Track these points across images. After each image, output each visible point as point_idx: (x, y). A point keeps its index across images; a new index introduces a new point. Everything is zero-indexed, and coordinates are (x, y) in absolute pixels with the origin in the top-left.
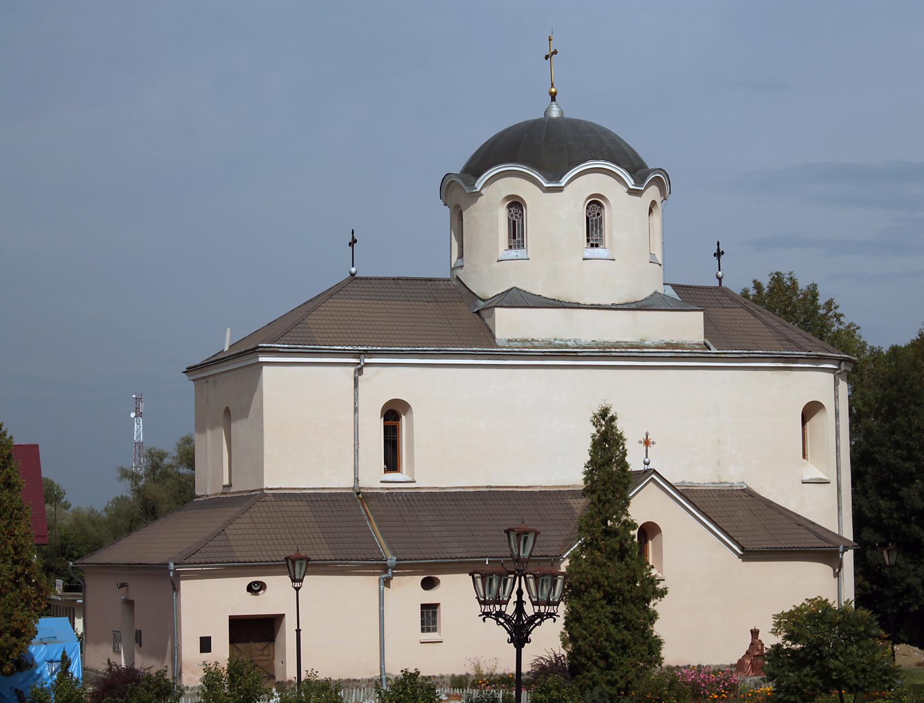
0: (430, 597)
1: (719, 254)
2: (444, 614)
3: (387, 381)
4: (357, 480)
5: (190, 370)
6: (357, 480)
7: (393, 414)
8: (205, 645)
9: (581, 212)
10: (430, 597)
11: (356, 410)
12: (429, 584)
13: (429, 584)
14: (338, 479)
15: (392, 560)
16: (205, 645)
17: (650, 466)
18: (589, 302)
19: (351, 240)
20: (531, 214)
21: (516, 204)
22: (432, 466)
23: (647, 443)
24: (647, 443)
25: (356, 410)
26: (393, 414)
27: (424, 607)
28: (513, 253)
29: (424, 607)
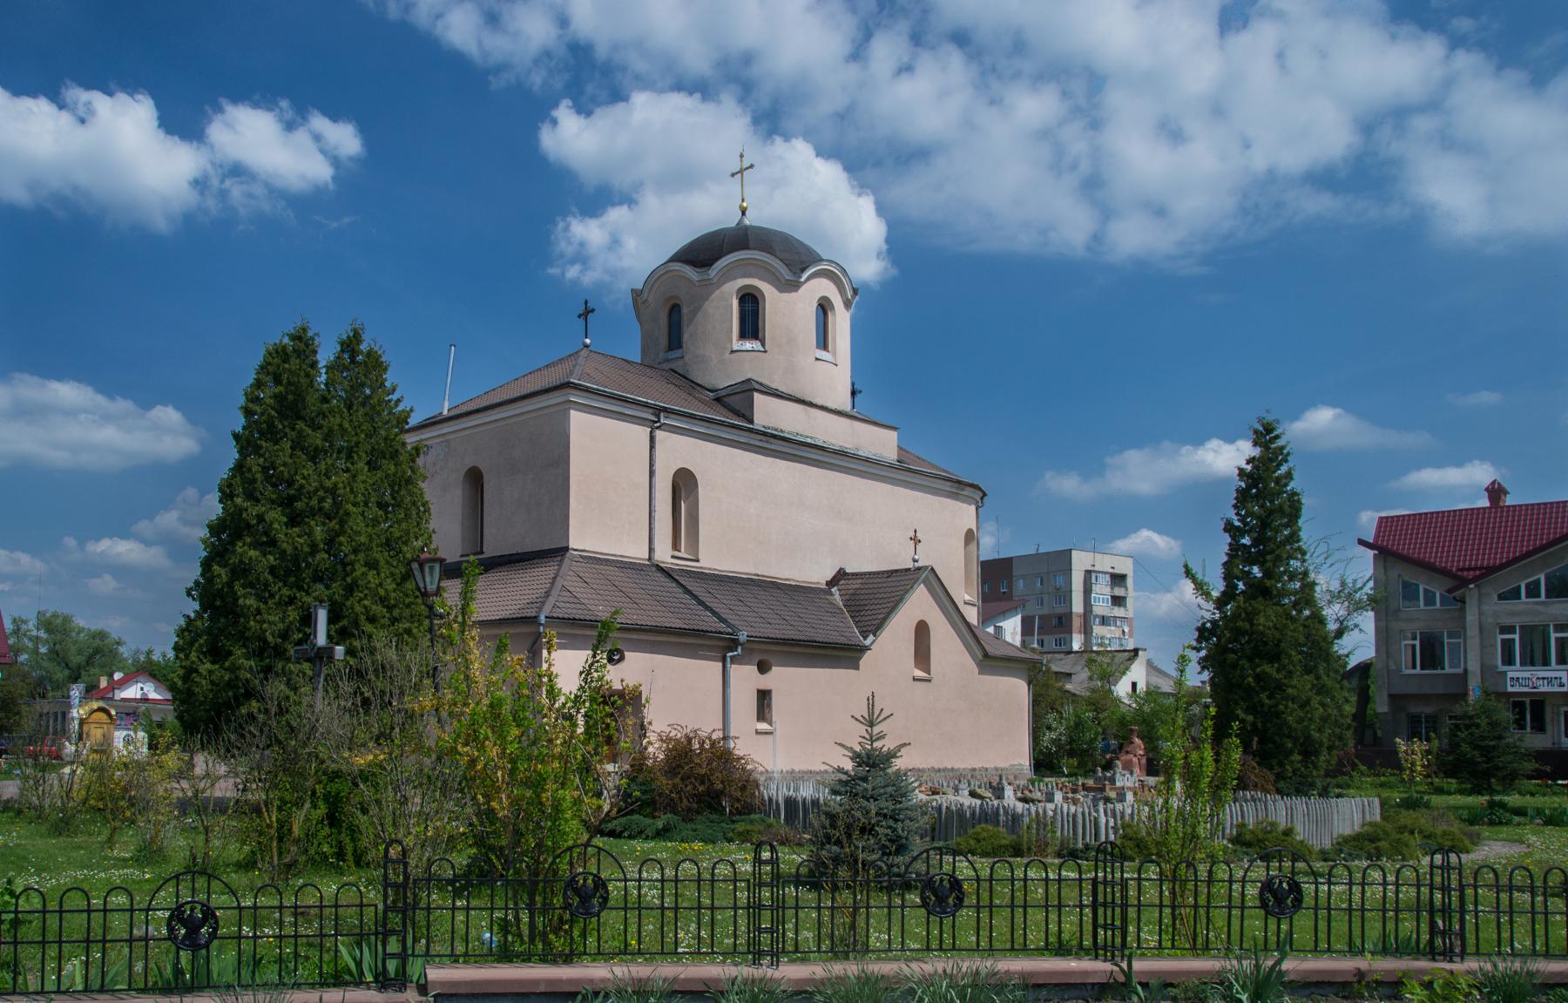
0: (765, 681)
2: (776, 700)
3: (678, 450)
4: (651, 550)
6: (651, 550)
7: (684, 484)
10: (765, 681)
11: (652, 473)
12: (763, 668)
13: (763, 668)
19: (581, 310)
23: (916, 540)
24: (916, 540)
27: (759, 692)
28: (748, 345)
29: (759, 692)
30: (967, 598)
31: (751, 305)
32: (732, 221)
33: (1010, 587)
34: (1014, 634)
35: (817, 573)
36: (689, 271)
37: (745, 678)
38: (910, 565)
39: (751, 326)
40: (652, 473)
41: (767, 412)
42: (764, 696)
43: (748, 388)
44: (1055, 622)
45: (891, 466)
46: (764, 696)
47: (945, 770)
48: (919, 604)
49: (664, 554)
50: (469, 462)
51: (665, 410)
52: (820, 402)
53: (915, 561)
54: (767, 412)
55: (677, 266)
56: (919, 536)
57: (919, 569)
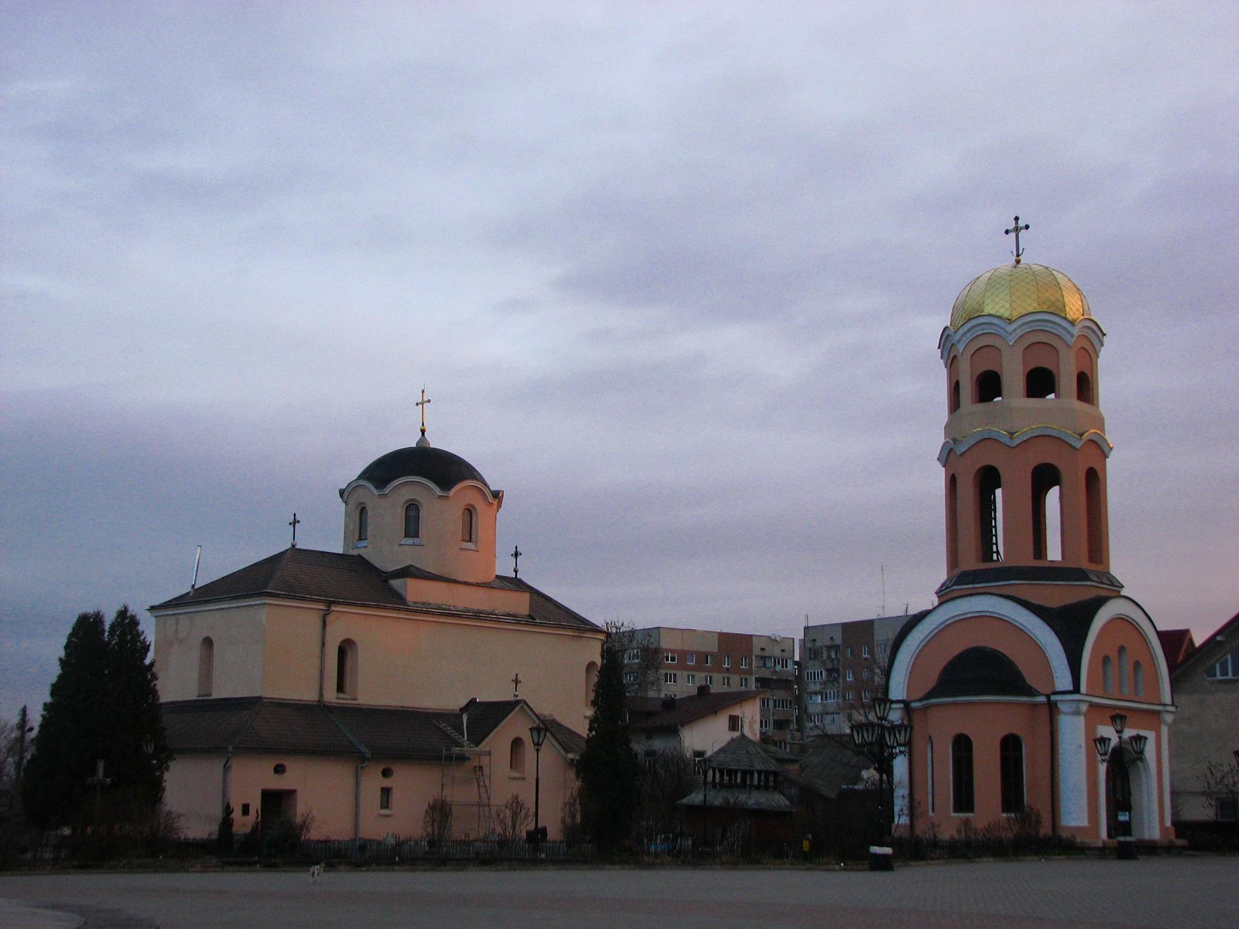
0: (387, 783)
1: (516, 555)
2: (396, 796)
4: (321, 695)
5: (152, 608)
6: (321, 695)
7: (346, 648)
8: (246, 809)
9: (401, 512)
10: (387, 783)
12: (386, 773)
13: (386, 773)
14: (308, 695)
15: (368, 755)
16: (246, 809)
19: (292, 520)
20: (423, 514)
22: (375, 688)
23: (517, 681)
24: (517, 681)
25: (323, 645)
26: (346, 648)
27: (383, 789)
28: (410, 541)
29: (383, 789)
31: (412, 512)
32: (410, 441)
33: (871, 652)
34: (752, 721)
35: (455, 702)
37: (372, 782)
38: (512, 699)
39: (412, 527)
41: (414, 590)
42: (386, 792)
43: (406, 572)
46: (386, 792)
48: (515, 727)
49: (331, 696)
50: (205, 633)
52: (461, 578)
55: (362, 482)
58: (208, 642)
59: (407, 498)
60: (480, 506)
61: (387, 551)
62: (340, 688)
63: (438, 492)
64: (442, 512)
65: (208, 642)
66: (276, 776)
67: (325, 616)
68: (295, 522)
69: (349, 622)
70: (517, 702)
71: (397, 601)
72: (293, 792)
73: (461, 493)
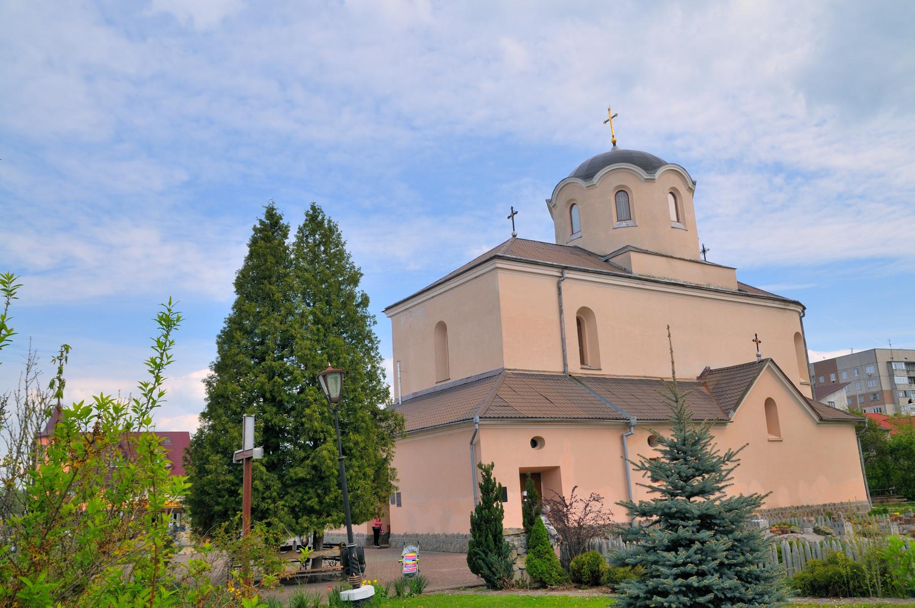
1: (704, 251)
4: (565, 365)
5: (387, 309)
6: (565, 365)
7: (583, 318)
11: (561, 312)
14: (554, 366)
15: (634, 421)
17: (762, 358)
18: (678, 256)
21: (622, 192)
23: (757, 341)
24: (757, 341)
26: (583, 318)
28: (624, 224)
30: (802, 381)
36: (580, 182)
38: (756, 359)
40: (561, 312)
43: (626, 250)
44: (871, 398)
45: (733, 294)
47: (802, 507)
48: (764, 386)
49: (574, 367)
51: (566, 268)
53: (758, 356)
54: (639, 264)
56: (759, 339)
57: (762, 361)
58: (442, 327)
59: (614, 185)
60: (682, 190)
61: (603, 237)
62: (583, 362)
63: (645, 175)
64: (649, 196)
65: (442, 327)
66: (534, 451)
67: (559, 283)
68: (514, 213)
69: (582, 291)
70: (762, 362)
71: (625, 273)
72: (554, 470)
73: (663, 180)
